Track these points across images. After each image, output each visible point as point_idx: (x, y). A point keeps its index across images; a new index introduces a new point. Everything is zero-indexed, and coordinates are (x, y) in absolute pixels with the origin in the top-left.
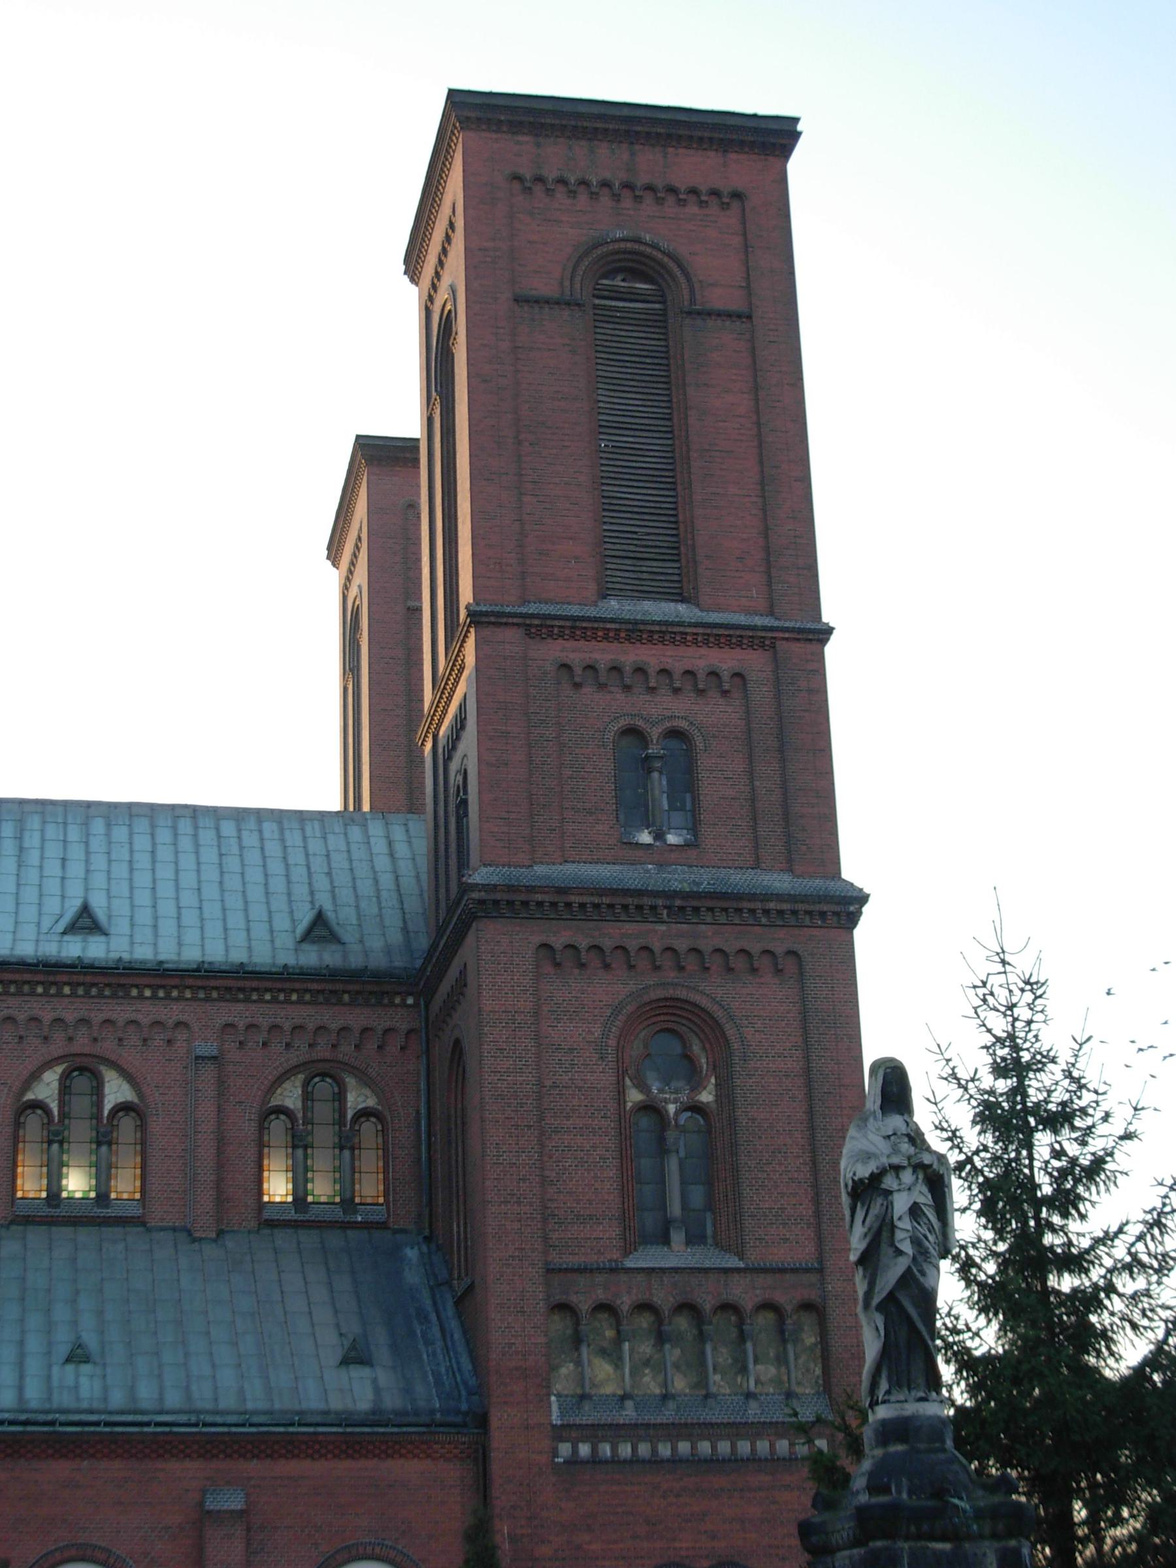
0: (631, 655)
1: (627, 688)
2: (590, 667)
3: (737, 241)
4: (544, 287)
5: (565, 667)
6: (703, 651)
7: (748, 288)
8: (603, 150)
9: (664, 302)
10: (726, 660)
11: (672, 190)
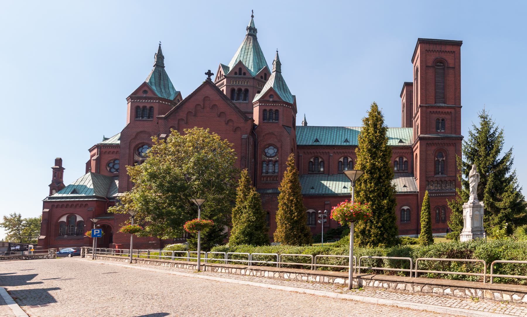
0: (438, 110)
1: (438, 114)
2: (434, 112)
5: (431, 112)
6: (447, 109)
10: (449, 110)
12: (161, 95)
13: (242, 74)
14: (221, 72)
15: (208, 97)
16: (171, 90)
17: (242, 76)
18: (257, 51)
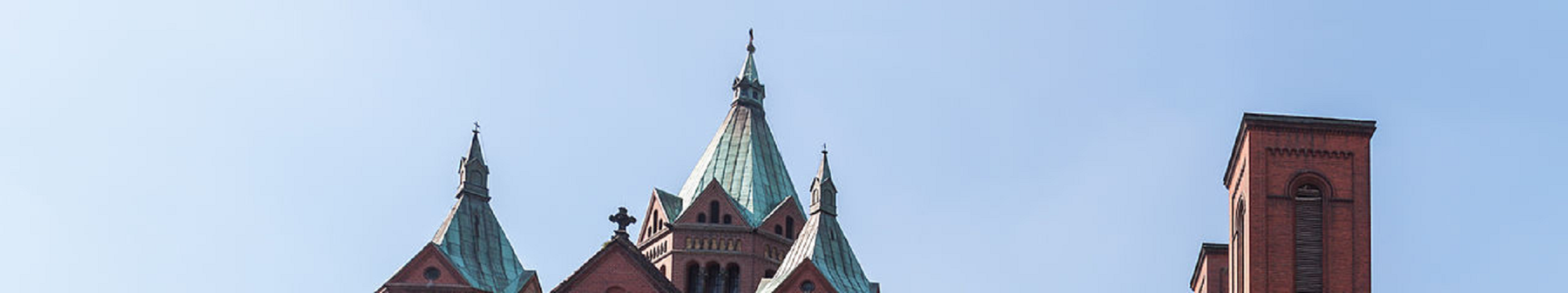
3: (1350, 172)
4: (1277, 192)
7: (1353, 191)
8: (1301, 137)
9: (1321, 196)
11: (1326, 152)
12: (480, 283)
13: (721, 220)
14: (656, 212)
15: (617, 288)
16: (508, 267)
17: (720, 225)
18: (766, 151)
